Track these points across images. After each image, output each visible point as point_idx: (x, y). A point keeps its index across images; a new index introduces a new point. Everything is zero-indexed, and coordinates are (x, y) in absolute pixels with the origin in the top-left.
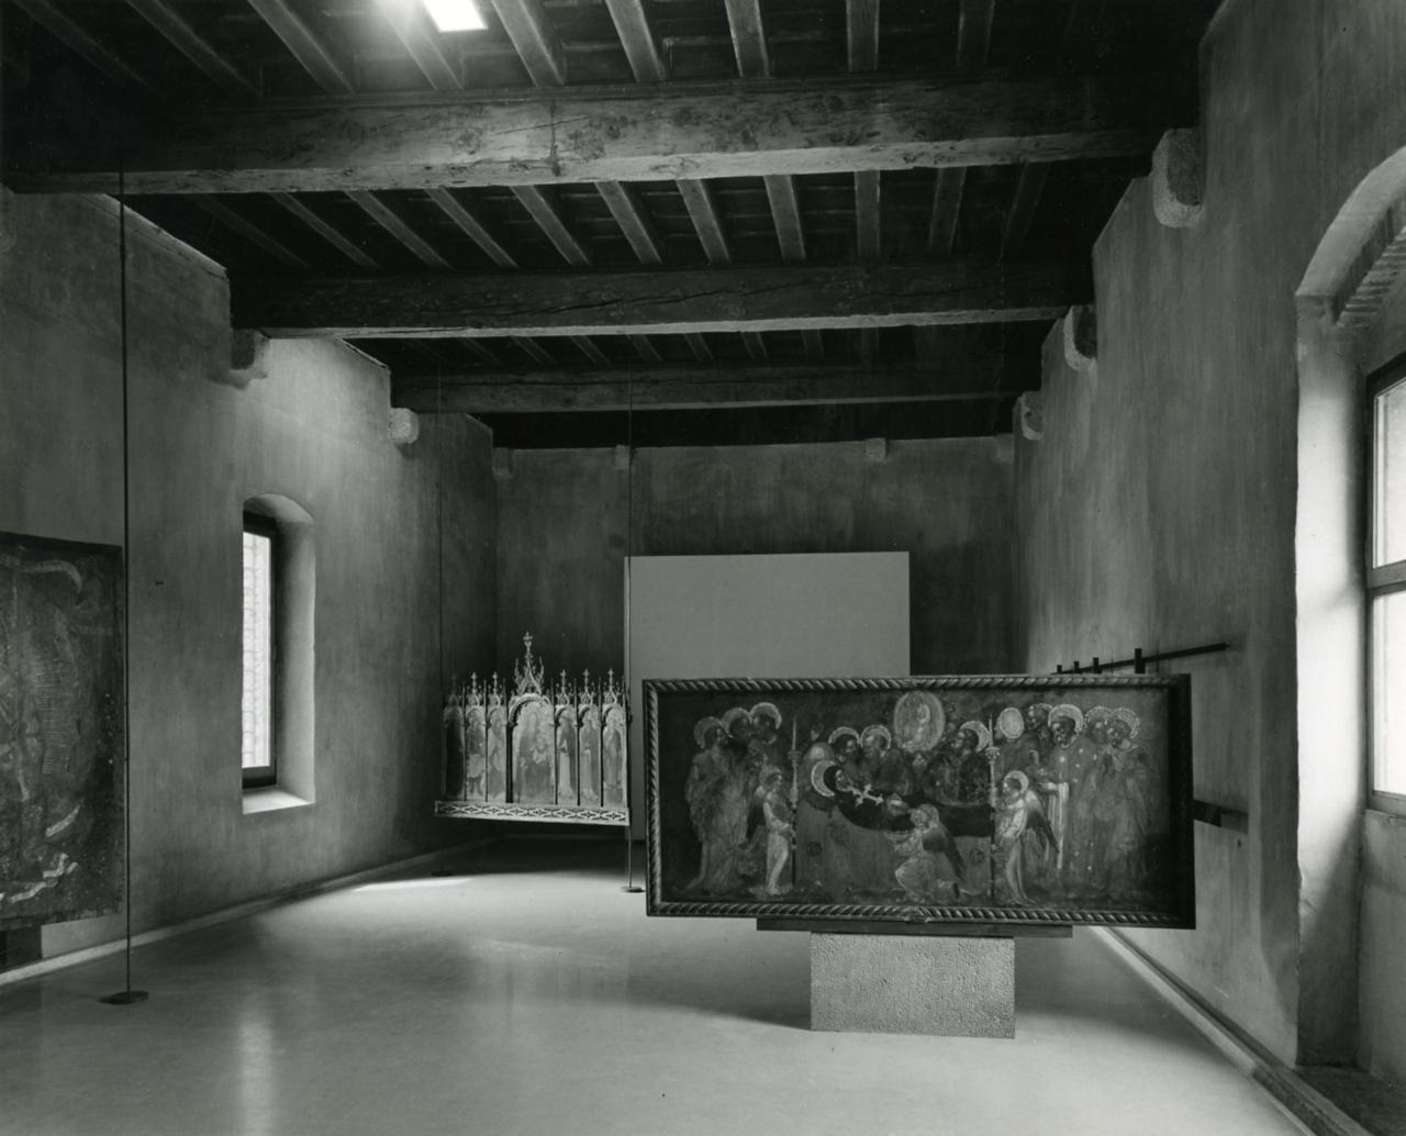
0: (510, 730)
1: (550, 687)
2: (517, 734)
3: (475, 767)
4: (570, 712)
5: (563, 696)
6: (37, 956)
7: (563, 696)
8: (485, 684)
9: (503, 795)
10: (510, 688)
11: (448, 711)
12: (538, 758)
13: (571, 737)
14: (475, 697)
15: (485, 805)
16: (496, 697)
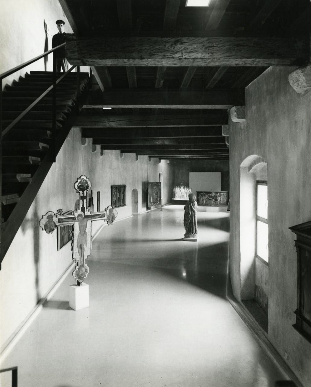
0: (180, 192)
1: (184, 188)
2: (181, 192)
3: (176, 195)
4: (186, 190)
5: (185, 189)
6: (151, 209)
7: (185, 189)
8: (177, 187)
9: (179, 198)
10: (180, 188)
11: (174, 190)
12: (183, 194)
13: (186, 193)
14: (176, 189)
15: (177, 198)
16: (179, 189)
